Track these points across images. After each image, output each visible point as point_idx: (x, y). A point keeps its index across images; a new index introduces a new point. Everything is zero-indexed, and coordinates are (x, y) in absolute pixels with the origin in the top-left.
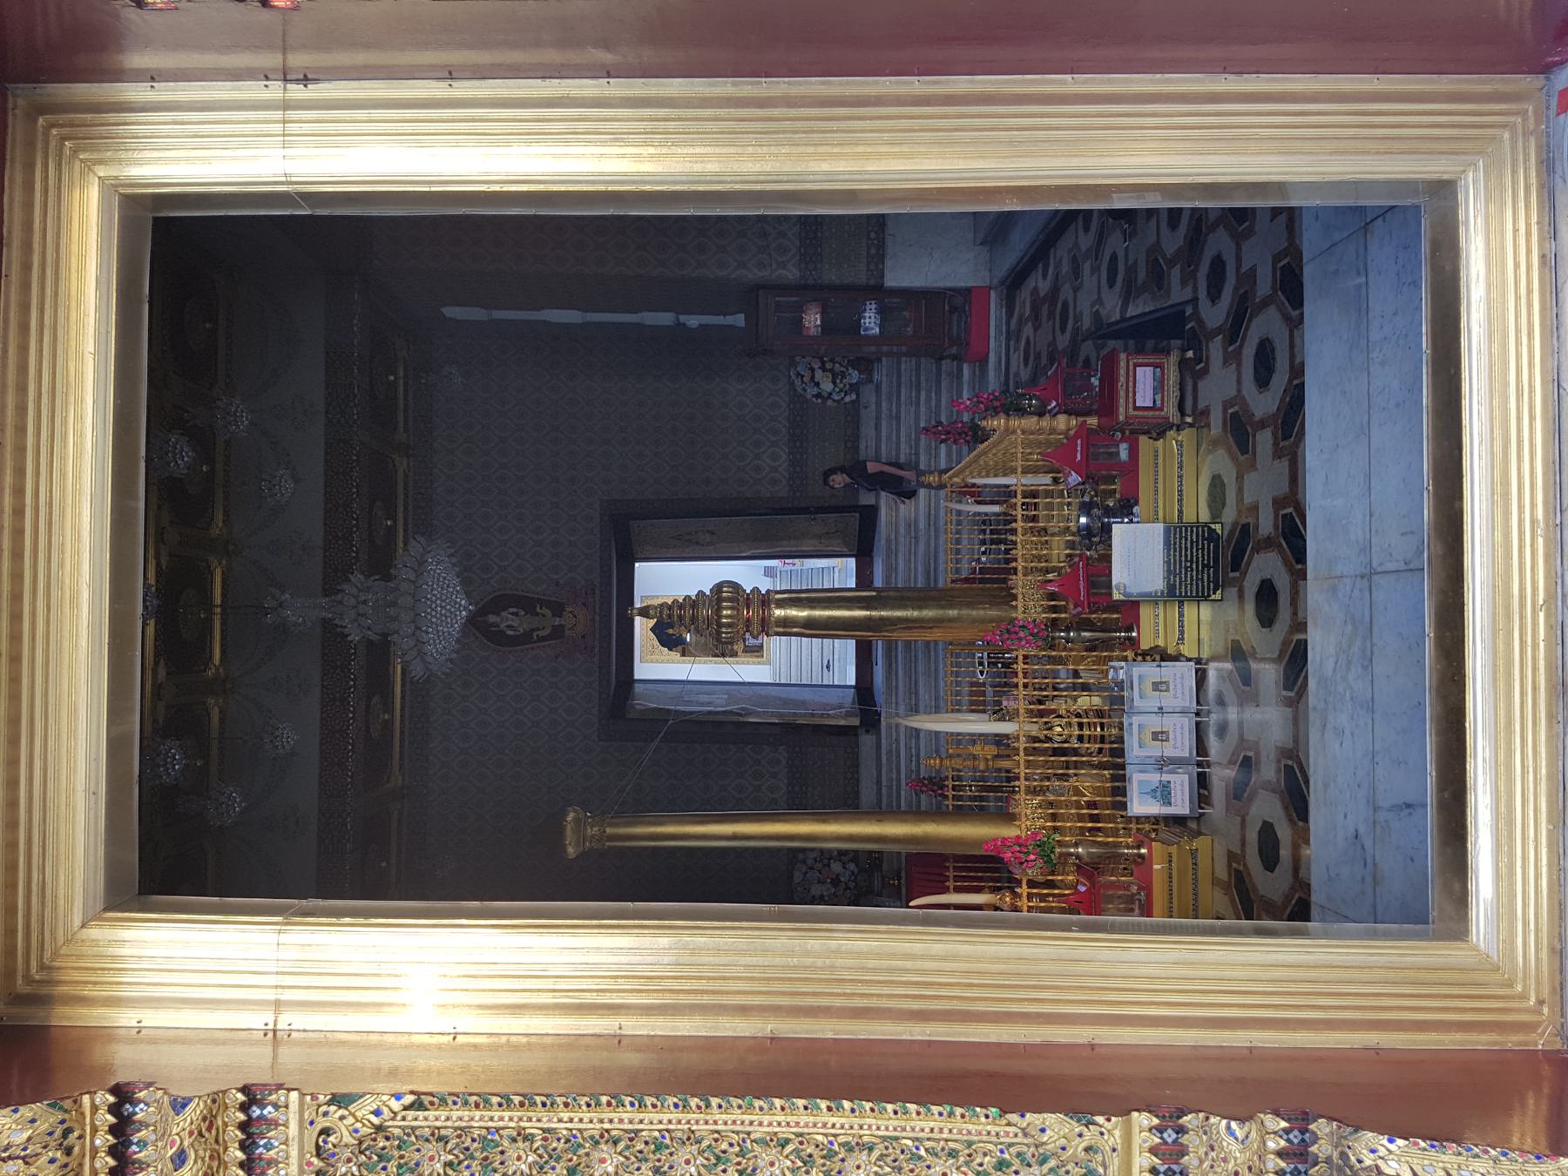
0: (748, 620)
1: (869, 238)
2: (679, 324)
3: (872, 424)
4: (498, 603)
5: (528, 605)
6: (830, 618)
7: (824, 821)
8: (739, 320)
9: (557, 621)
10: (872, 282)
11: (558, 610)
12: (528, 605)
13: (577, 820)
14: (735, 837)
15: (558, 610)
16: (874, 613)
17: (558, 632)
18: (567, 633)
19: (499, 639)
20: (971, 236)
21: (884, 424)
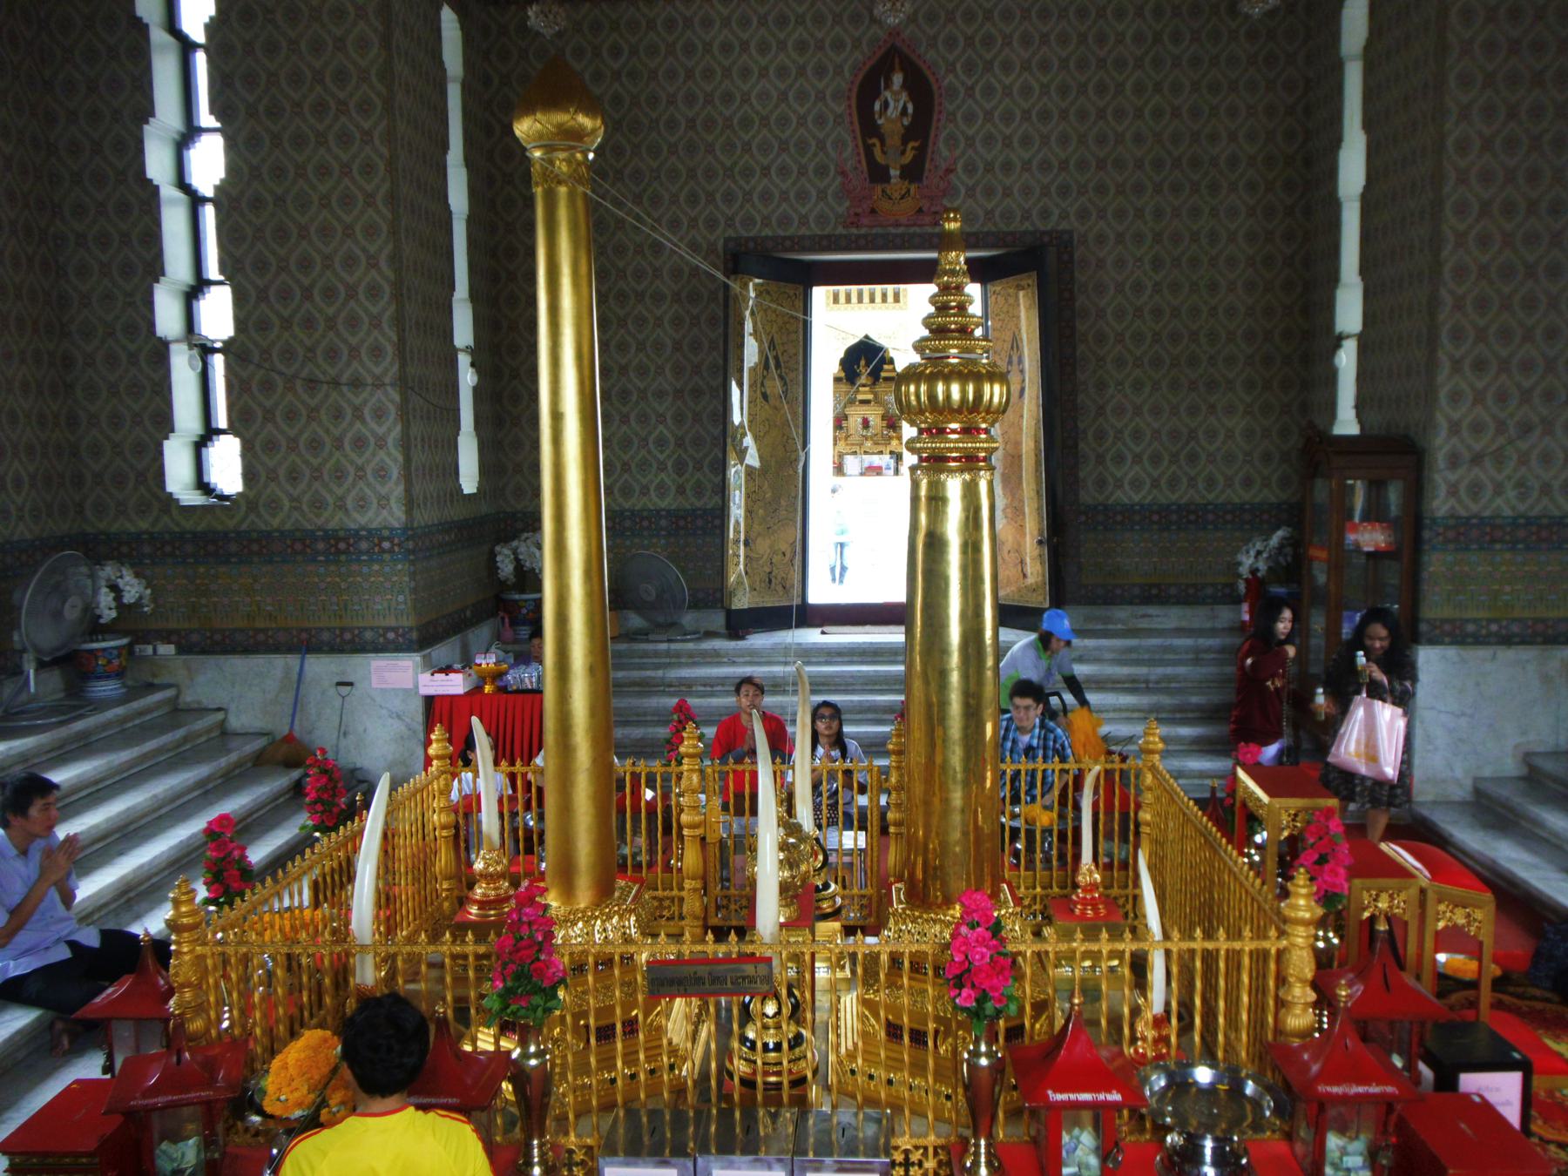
0: (942, 431)
1: (1490, 621)
2: (1338, 341)
3: (1184, 624)
4: (920, 89)
5: (919, 128)
6: (946, 579)
7: (588, 574)
8: (1347, 423)
9: (894, 172)
10: (1423, 627)
12: (919, 128)
13: (577, 135)
14: (557, 417)
15: (912, 173)
16: (955, 659)
17: (878, 174)
18: (879, 188)
19: (869, 90)
20: (1487, 772)
21: (1188, 642)
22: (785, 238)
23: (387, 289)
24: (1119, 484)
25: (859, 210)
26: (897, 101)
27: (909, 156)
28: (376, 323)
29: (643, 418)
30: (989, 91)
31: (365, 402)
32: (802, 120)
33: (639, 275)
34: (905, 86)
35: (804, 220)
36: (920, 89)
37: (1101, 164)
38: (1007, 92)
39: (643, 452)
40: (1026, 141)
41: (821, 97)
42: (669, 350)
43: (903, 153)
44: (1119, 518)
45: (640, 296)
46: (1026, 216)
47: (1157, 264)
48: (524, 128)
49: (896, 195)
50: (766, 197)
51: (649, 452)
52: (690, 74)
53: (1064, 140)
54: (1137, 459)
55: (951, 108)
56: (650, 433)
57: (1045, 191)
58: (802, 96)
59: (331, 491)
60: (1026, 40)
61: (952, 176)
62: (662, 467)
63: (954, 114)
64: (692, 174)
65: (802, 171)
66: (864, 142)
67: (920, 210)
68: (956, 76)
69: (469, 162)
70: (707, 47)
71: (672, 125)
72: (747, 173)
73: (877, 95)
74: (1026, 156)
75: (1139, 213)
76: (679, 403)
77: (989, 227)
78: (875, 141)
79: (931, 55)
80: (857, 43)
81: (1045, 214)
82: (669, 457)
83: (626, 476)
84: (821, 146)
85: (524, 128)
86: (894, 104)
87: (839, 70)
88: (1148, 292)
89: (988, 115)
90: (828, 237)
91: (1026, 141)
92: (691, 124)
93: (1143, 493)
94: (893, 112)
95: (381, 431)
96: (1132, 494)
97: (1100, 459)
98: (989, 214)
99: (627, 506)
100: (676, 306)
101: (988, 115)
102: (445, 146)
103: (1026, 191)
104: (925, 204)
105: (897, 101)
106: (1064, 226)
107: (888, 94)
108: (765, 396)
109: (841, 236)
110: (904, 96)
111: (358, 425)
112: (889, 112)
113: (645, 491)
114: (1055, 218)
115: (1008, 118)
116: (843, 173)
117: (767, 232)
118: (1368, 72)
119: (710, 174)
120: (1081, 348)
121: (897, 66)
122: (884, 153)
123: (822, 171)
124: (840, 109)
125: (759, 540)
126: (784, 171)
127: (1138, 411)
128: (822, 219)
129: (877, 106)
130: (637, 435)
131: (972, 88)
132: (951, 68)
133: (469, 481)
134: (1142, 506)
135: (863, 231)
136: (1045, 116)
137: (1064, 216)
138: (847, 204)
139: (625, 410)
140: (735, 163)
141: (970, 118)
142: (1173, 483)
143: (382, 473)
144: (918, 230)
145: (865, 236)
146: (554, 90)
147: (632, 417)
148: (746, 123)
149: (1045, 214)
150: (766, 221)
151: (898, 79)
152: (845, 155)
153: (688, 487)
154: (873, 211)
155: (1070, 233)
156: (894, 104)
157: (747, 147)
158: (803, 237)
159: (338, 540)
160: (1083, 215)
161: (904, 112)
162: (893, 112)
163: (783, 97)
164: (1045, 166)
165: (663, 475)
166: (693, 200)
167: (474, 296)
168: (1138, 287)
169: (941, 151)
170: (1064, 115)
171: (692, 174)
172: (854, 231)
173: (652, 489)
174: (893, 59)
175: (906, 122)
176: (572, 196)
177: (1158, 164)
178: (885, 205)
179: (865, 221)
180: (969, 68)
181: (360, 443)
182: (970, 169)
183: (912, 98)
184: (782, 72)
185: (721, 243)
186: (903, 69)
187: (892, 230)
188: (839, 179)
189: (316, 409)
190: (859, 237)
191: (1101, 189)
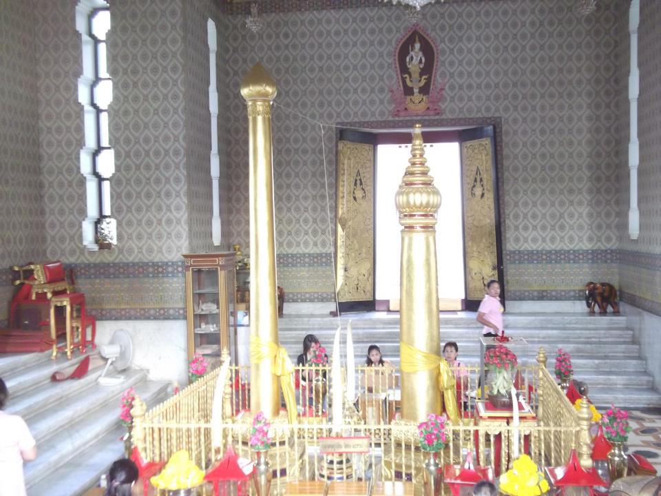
4: (428, 50)
5: (427, 69)
9: (416, 90)
11: (425, 90)
12: (427, 69)
15: (425, 90)
17: (408, 91)
18: (409, 98)
19: (404, 52)
23: (183, 151)
24: (526, 240)
25: (399, 109)
26: (417, 57)
27: (423, 82)
28: (177, 167)
29: (298, 209)
30: (461, 51)
31: (172, 203)
32: (372, 66)
33: (296, 141)
34: (421, 49)
35: (373, 114)
36: (428, 50)
37: (515, 85)
38: (469, 51)
39: (298, 226)
40: (478, 74)
41: (381, 55)
43: (420, 81)
44: (526, 257)
45: (296, 151)
46: (479, 110)
47: (543, 132)
48: (245, 92)
51: (300, 226)
52: (320, 45)
53: (497, 74)
54: (535, 228)
55: (443, 59)
57: (488, 98)
58: (372, 55)
59: (156, 244)
60: (478, 26)
61: (443, 92)
62: (306, 234)
63: (444, 62)
64: (321, 92)
65: (372, 91)
66: (402, 77)
67: (428, 108)
68: (445, 44)
69: (219, 89)
70: (329, 32)
71: (312, 70)
72: (347, 92)
73: (408, 53)
74: (479, 81)
75: (534, 109)
76: (315, 202)
77: (461, 116)
78: (406, 75)
79: (433, 34)
81: (488, 109)
84: (381, 78)
85: (245, 92)
86: (416, 58)
87: (390, 42)
88: (539, 146)
89: (460, 62)
91: (478, 74)
92: (321, 69)
93: (538, 245)
94: (415, 61)
95: (178, 216)
96: (533, 245)
97: (517, 228)
98: (461, 109)
99: (290, 252)
101: (460, 62)
102: (208, 83)
103: (479, 98)
104: (431, 106)
105: (417, 57)
106: (497, 115)
108: (355, 198)
109: (390, 121)
110: (421, 53)
111: (169, 214)
114: (493, 111)
115: (470, 63)
116: (392, 91)
118: (640, 39)
120: (506, 174)
121: (417, 40)
122: (411, 81)
123: (382, 90)
124: (390, 61)
125: (352, 269)
126: (364, 90)
127: (535, 205)
129: (408, 59)
131: (453, 49)
132: (443, 41)
133: (217, 239)
134: (538, 251)
135: (401, 119)
136: (488, 62)
137: (497, 110)
138: (394, 106)
139: (289, 205)
140: (341, 87)
141: (452, 64)
142: (553, 240)
143: (179, 236)
144: (427, 118)
145: (402, 121)
146: (257, 76)
149: (488, 109)
151: (417, 46)
152: (393, 82)
153: (318, 243)
154: (406, 109)
155: (500, 117)
156: (416, 58)
157: (347, 80)
158: (372, 122)
159: (159, 267)
160: (506, 109)
161: (420, 61)
162: (415, 61)
163: (364, 56)
164: (488, 86)
165: (307, 237)
166: (321, 105)
167: (220, 152)
168: (534, 144)
169: (438, 80)
170: (497, 62)
171: (321, 92)
172: (397, 119)
174: (414, 36)
175: (422, 66)
176: (264, 118)
177: (543, 84)
178: (411, 106)
180: (451, 40)
181: (169, 222)
182: (452, 88)
183: (425, 54)
184: (364, 44)
186: (420, 41)
188: (390, 94)
189: (150, 206)
190: (399, 121)
191: (515, 97)
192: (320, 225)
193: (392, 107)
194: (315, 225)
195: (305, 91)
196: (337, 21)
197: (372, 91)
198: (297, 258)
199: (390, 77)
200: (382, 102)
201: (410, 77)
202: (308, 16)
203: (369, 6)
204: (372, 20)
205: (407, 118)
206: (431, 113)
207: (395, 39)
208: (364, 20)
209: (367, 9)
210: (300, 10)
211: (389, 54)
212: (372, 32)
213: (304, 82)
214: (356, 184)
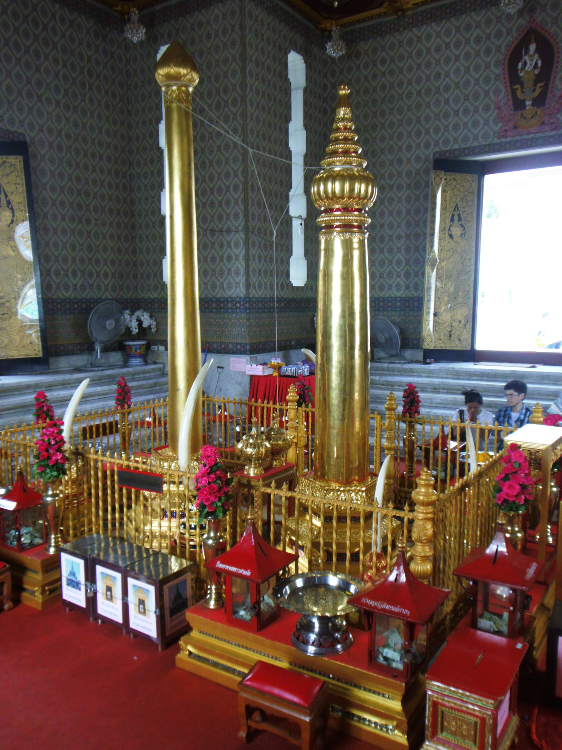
4: (547, 52)
5: (545, 75)
9: (528, 103)
18: (519, 113)
22: (465, 149)
25: (507, 128)
26: (532, 60)
29: (390, 250)
33: (391, 176)
34: (536, 51)
36: (547, 52)
39: (390, 267)
41: (488, 66)
42: (404, 214)
43: (534, 90)
49: (529, 116)
50: (456, 127)
51: (393, 268)
56: (394, 258)
62: (399, 276)
71: (409, 95)
72: (447, 115)
73: (520, 58)
76: (408, 241)
78: (517, 86)
80: (509, 32)
82: (402, 270)
83: (381, 280)
86: (531, 62)
87: (498, 48)
90: (489, 145)
99: (381, 295)
100: (408, 191)
107: (526, 58)
108: (451, 236)
109: (496, 144)
110: (536, 56)
112: (527, 68)
113: (390, 288)
116: (499, 108)
117: (456, 146)
119: (427, 119)
121: (533, 40)
122: (523, 92)
124: (498, 71)
125: (444, 313)
128: (486, 136)
129: (520, 66)
130: (387, 258)
135: (509, 139)
138: (500, 125)
139: (382, 246)
147: (386, 249)
148: (447, 88)
150: (456, 140)
151: (533, 47)
152: (500, 97)
153: (411, 285)
156: (531, 62)
162: (528, 68)
165: (399, 279)
166: (418, 134)
172: (504, 140)
173: (394, 286)
175: (536, 72)
179: (511, 133)
183: (541, 57)
184: (467, 56)
185: (431, 156)
186: (536, 41)
187: (525, 137)
190: (506, 143)
192: (413, 267)
193: (497, 128)
194: (408, 267)
195: (402, 121)
196: (438, 35)
197: (476, 111)
198: (389, 302)
199: (497, 92)
200: (486, 122)
201: (522, 87)
202: (406, 35)
203: (475, 10)
204: (478, 26)
205: (516, 138)
206: (547, 128)
207: (508, 41)
208: (468, 28)
209: (473, 14)
210: (399, 30)
211: (497, 64)
212: (478, 40)
213: (400, 111)
214: (452, 220)
